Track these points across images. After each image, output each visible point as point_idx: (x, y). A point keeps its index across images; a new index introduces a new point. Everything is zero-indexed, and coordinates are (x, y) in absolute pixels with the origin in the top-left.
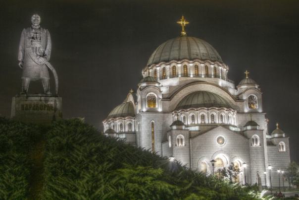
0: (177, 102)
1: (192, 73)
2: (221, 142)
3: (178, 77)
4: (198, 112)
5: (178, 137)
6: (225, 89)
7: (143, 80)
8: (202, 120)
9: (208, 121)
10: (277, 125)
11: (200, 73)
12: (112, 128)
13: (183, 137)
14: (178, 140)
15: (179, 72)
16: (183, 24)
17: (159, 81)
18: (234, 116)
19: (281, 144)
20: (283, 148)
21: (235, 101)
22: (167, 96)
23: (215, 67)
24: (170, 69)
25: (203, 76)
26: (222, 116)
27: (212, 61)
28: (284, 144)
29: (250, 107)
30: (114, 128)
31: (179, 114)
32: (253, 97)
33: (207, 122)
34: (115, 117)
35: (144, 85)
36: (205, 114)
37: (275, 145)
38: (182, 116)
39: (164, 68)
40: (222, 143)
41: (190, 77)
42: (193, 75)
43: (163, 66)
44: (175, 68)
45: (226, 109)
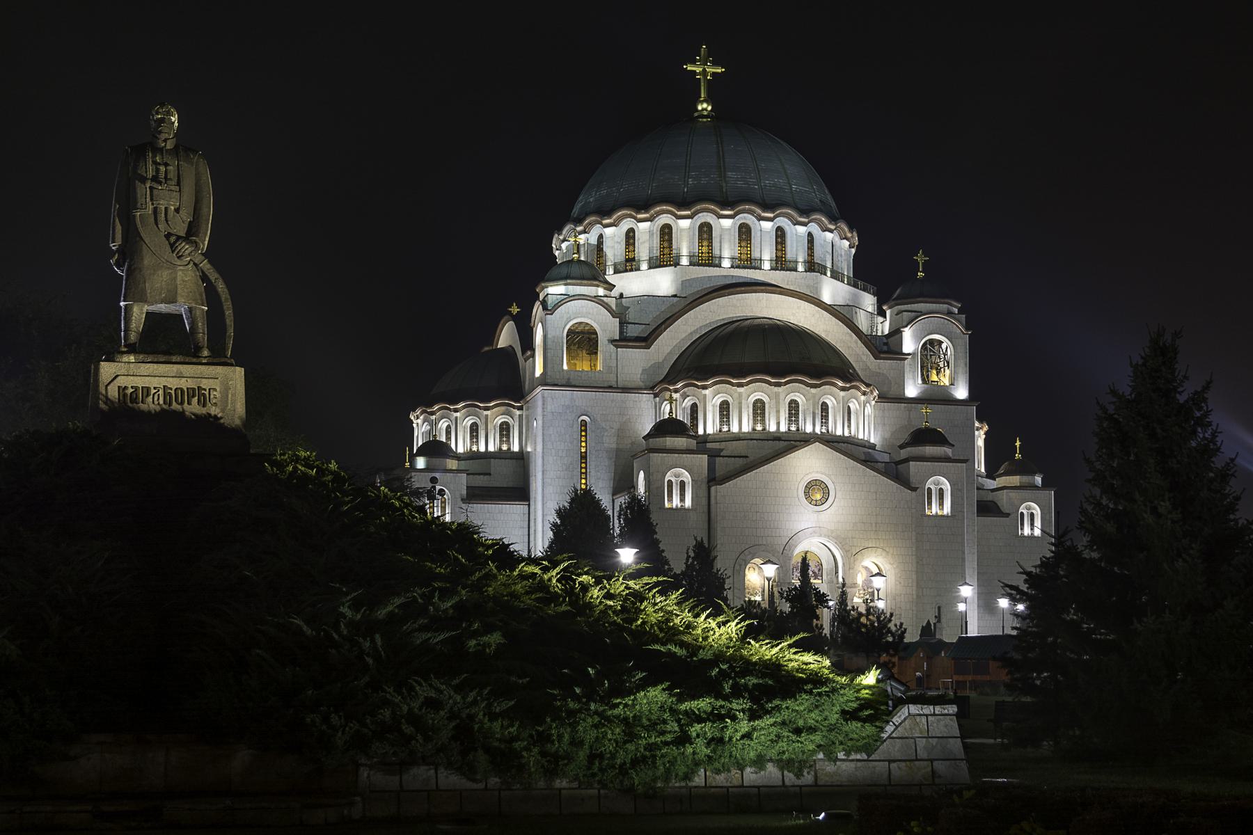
1: (727, 251)
2: (818, 496)
3: (677, 264)
4: (741, 390)
6: (843, 314)
7: (554, 272)
8: (755, 421)
9: (777, 423)
10: (1018, 444)
11: (756, 255)
12: (444, 439)
13: (686, 477)
15: (685, 246)
16: (704, 73)
17: (611, 277)
18: (869, 410)
19: (1025, 512)
21: (876, 359)
22: (632, 331)
23: (810, 235)
24: (651, 233)
25: (767, 266)
26: (825, 408)
28: (1037, 511)
29: (924, 381)
30: (448, 438)
31: (675, 396)
32: (940, 343)
33: (773, 428)
34: (452, 398)
35: (555, 290)
36: (766, 399)
37: (1007, 515)
38: (688, 402)
41: (719, 266)
42: (732, 258)
43: (627, 224)
44: (670, 234)
45: (840, 384)
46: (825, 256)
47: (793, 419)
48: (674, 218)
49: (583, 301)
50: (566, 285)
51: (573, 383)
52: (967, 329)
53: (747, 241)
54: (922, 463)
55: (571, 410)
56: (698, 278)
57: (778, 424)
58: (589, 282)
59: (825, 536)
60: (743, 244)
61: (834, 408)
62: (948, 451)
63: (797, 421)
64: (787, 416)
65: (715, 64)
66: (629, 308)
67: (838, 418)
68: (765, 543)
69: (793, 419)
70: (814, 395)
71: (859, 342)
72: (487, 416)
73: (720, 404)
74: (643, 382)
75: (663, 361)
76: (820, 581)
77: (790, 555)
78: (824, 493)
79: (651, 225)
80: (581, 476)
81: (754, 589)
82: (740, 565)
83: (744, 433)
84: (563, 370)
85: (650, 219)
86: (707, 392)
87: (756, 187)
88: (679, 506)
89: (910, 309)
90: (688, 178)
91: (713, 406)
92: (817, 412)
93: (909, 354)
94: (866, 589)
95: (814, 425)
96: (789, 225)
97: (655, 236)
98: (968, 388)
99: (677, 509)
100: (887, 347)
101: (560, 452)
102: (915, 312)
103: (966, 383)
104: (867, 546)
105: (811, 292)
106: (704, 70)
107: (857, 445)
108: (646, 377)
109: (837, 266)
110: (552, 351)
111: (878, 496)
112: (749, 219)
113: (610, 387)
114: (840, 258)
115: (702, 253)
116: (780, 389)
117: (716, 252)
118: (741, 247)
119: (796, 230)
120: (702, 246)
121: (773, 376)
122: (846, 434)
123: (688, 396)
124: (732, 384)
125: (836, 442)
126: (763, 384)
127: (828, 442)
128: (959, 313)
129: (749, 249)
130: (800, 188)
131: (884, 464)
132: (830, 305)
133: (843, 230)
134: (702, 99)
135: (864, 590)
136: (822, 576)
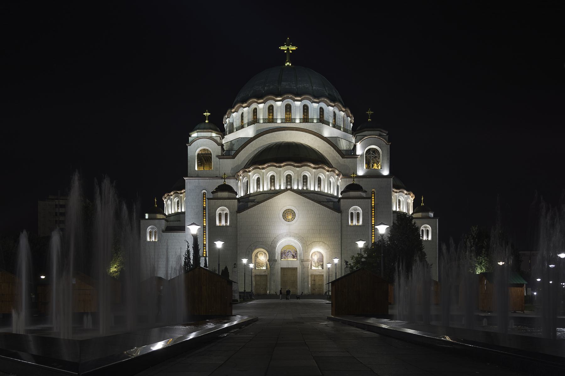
0: (244, 160)
1: (279, 116)
2: (290, 217)
4: (264, 171)
5: (218, 211)
8: (271, 186)
9: (280, 185)
13: (227, 211)
14: (220, 215)
20: (428, 235)
21: (343, 158)
24: (249, 113)
25: (298, 121)
27: (315, 97)
29: (368, 167)
36: (275, 175)
39: (243, 113)
40: (294, 218)
45: (312, 165)
46: (329, 118)
47: (289, 183)
48: (257, 104)
49: (204, 139)
50: (197, 132)
51: (200, 176)
52: (388, 142)
53: (290, 111)
54: (347, 200)
55: (198, 188)
56: (264, 128)
57: (280, 186)
58: (207, 130)
59: (293, 236)
60: (288, 113)
61: (310, 177)
62: (364, 195)
63: (291, 185)
64: (285, 182)
65: (293, 46)
66: (234, 144)
67: (312, 182)
68: (262, 240)
69: (289, 183)
70: (298, 171)
71: (335, 151)
72: (181, 196)
73: (257, 179)
74: (232, 174)
75: (241, 164)
76: (296, 259)
77: (274, 246)
78: (293, 215)
79: (248, 110)
80: (203, 217)
81: (262, 264)
82: (249, 252)
83: (265, 191)
84: (195, 170)
85: (248, 106)
86: (250, 174)
87: (295, 88)
88: (224, 225)
89: (362, 135)
90: (265, 87)
91: (254, 180)
92: (300, 179)
93: (359, 155)
94: (319, 263)
95: (298, 186)
96: (309, 103)
97: (250, 114)
98: (389, 170)
99: (223, 226)
100: (351, 153)
101: (193, 207)
102: (362, 136)
103: (388, 167)
104: (315, 241)
105: (317, 131)
106: (288, 48)
107: (322, 195)
108: (233, 172)
109: (337, 123)
110: (190, 162)
111: (321, 216)
112: (289, 101)
113: (217, 177)
114: (339, 120)
115: (270, 119)
116: (281, 169)
117: (275, 117)
118: (287, 114)
119: (313, 106)
120: (270, 116)
121: (277, 162)
122: (316, 190)
123: (245, 177)
124: (259, 168)
125: (305, 193)
126: (274, 167)
127: (301, 193)
128: (387, 135)
129: (291, 115)
130: (317, 88)
131: (332, 203)
132: (325, 137)
133: (340, 107)
134: (287, 60)
135: (318, 263)
136: (297, 257)
